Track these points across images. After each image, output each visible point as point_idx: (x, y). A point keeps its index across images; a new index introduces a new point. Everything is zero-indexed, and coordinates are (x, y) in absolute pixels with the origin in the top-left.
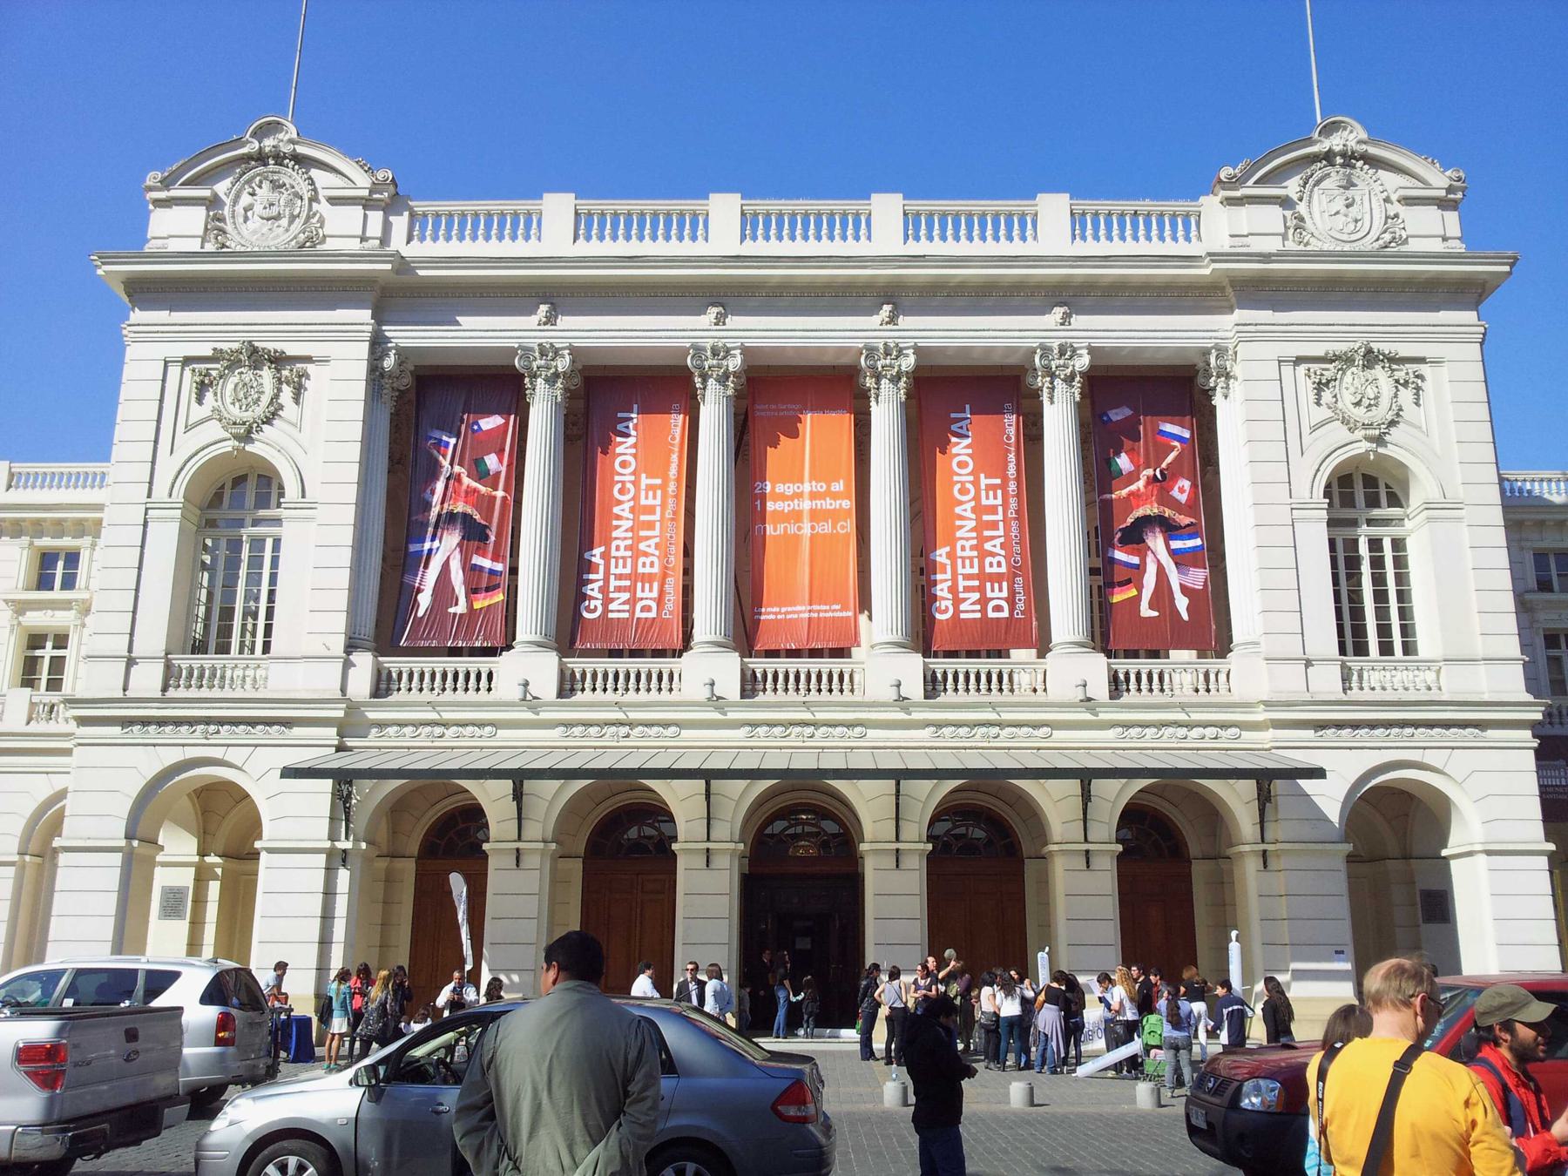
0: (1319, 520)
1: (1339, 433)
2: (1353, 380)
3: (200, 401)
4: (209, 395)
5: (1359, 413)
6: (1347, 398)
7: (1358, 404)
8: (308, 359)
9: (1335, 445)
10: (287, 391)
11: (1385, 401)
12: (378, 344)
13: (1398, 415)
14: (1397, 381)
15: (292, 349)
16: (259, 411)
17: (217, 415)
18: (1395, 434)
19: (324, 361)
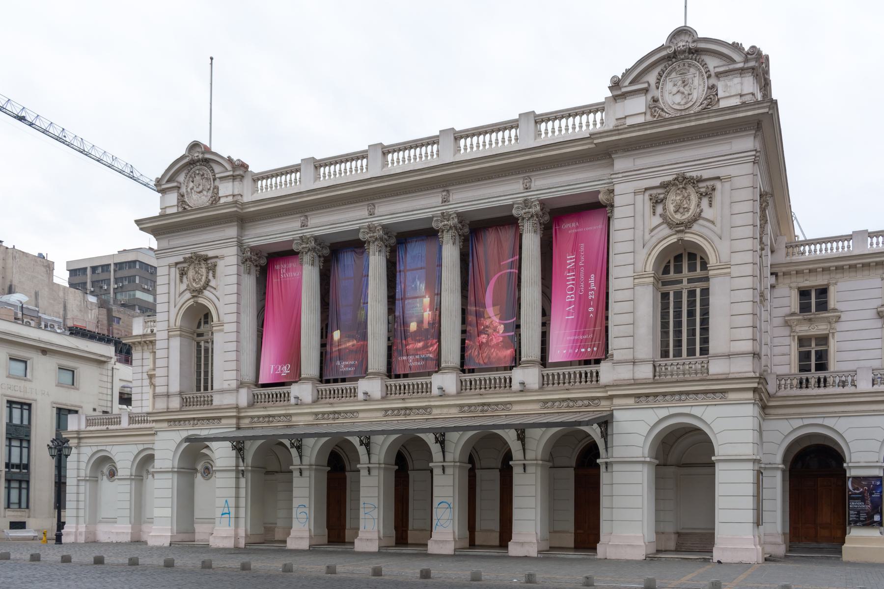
0: (648, 284)
1: (665, 231)
2: (673, 199)
3: (181, 281)
4: (185, 277)
5: (678, 217)
6: (671, 208)
7: (676, 212)
8: (217, 257)
9: (667, 238)
10: (211, 272)
11: (693, 206)
12: (240, 244)
13: (700, 214)
14: (701, 194)
15: (211, 254)
16: (202, 283)
17: (188, 289)
18: (696, 227)
19: (223, 257)
